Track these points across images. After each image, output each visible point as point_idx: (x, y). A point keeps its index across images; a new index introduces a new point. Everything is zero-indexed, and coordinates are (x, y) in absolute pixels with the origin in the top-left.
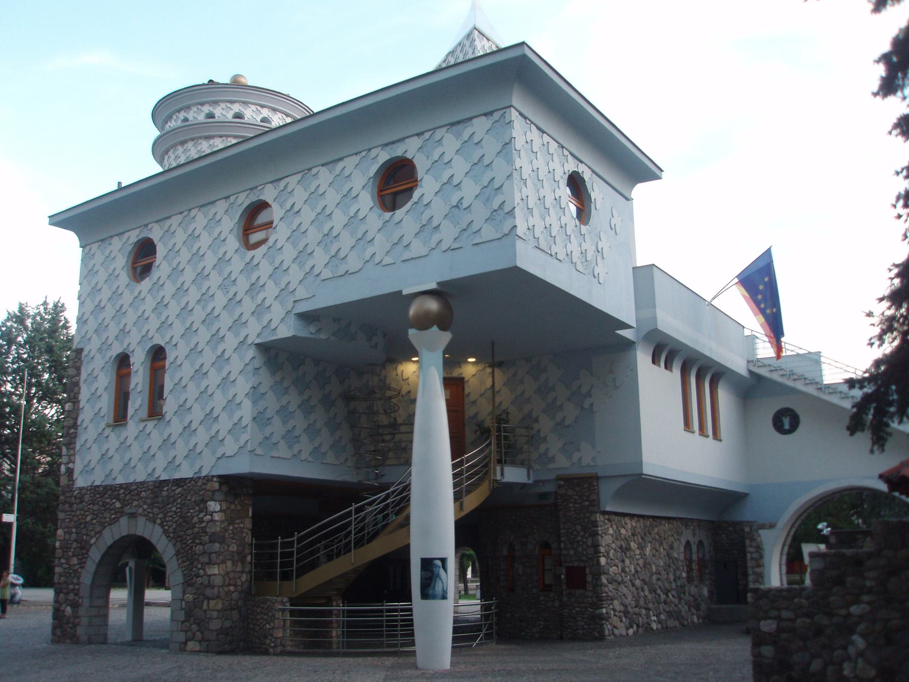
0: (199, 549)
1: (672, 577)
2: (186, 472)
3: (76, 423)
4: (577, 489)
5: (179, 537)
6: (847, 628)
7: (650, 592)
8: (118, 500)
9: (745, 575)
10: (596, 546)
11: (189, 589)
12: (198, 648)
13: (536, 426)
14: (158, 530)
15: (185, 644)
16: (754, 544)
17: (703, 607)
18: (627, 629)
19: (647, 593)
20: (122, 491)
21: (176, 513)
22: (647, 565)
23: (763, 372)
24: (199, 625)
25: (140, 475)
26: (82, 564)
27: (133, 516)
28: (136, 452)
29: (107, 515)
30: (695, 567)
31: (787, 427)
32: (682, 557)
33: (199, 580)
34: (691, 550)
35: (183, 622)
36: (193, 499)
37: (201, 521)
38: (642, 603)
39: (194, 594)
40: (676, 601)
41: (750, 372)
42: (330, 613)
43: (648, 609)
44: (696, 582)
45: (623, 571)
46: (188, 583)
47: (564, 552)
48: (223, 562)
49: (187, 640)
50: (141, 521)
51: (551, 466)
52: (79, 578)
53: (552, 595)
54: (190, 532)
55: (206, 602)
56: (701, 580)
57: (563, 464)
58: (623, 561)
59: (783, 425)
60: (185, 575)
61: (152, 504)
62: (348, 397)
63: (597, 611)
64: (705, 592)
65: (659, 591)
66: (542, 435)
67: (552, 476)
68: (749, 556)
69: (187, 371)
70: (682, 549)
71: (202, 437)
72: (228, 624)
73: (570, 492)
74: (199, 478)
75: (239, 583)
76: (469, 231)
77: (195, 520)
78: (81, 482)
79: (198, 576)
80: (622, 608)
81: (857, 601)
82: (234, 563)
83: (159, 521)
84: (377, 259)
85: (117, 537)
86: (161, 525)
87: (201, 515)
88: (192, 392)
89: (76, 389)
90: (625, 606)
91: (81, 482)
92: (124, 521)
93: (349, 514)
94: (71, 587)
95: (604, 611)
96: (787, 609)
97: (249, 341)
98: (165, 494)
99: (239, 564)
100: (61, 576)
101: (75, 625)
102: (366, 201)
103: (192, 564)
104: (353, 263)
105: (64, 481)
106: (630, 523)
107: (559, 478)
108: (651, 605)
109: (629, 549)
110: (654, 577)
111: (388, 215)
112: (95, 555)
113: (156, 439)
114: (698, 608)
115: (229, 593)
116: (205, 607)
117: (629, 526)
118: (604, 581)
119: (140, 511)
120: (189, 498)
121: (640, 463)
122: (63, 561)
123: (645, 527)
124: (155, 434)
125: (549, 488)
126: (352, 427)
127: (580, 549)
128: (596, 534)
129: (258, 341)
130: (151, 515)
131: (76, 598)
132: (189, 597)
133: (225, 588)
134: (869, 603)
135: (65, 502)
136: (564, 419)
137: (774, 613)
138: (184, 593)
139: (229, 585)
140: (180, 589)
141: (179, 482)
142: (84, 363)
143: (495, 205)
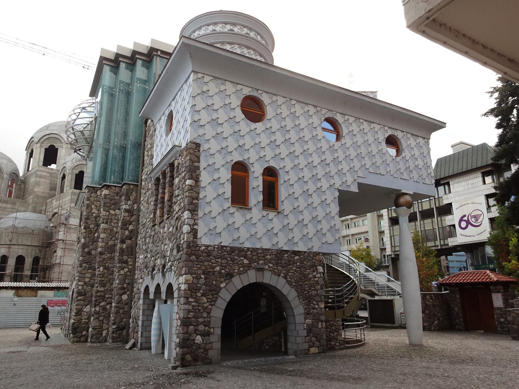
0: (314, 293)
2: (301, 247)
5: (300, 285)
12: (317, 352)
15: (308, 350)
20: (249, 253)
24: (316, 337)
25: (266, 244)
26: (213, 302)
27: (260, 270)
35: (305, 337)
36: (308, 264)
37: (315, 277)
39: (312, 319)
46: (307, 314)
49: (310, 347)
52: (209, 313)
55: (320, 323)
60: (305, 309)
61: (277, 264)
74: (311, 252)
77: (311, 276)
79: (314, 308)
83: (282, 275)
86: (285, 277)
87: (315, 274)
94: (201, 320)
101: (206, 350)
103: (309, 301)
119: (267, 267)
120: (305, 263)
124: (275, 220)
129: (340, 188)
130: (276, 271)
131: (207, 328)
138: (305, 319)
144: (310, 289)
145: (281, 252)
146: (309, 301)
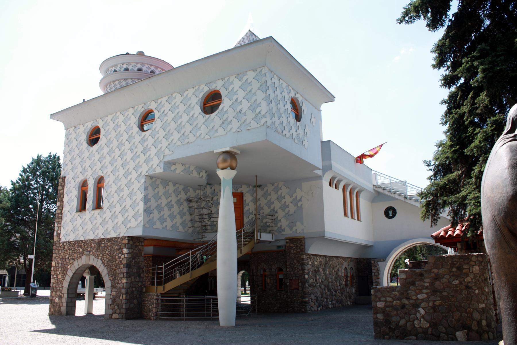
1: (338, 284)
2: (113, 235)
3: (62, 212)
4: (295, 244)
6: (416, 306)
7: (328, 291)
8: (81, 247)
9: (372, 283)
10: (303, 270)
11: (114, 290)
12: (118, 317)
13: (276, 215)
14: (100, 262)
15: (112, 315)
16: (375, 269)
17: (353, 297)
18: (318, 308)
19: (327, 291)
21: (108, 254)
22: (327, 278)
23: (380, 190)
26: (64, 278)
28: (90, 226)
29: (76, 255)
30: (349, 279)
31: (391, 215)
32: (343, 275)
33: (119, 286)
34: (347, 272)
37: (120, 258)
38: (324, 295)
40: (340, 295)
41: (374, 190)
42: (180, 301)
43: (327, 299)
44: (349, 286)
45: (316, 281)
46: (113, 287)
47: (289, 273)
48: (130, 277)
50: (92, 257)
51: (283, 233)
53: (283, 292)
54: (114, 263)
56: (352, 286)
57: (288, 233)
58: (316, 277)
59: (389, 215)
60: (112, 283)
62: (189, 201)
63: (304, 300)
64: (354, 291)
65: (332, 290)
66: (279, 219)
67: (284, 238)
68: (373, 274)
69: (114, 188)
70: (343, 271)
71: (120, 219)
72: (132, 306)
73: (292, 245)
74: (119, 238)
75: (137, 286)
76: (245, 124)
77: (117, 257)
78: (63, 240)
79: (118, 283)
80: (315, 298)
81: (421, 293)
82: (135, 278)
83: (100, 258)
84: (202, 137)
85: (80, 265)
86: (102, 260)
87: (120, 255)
88: (116, 198)
89: (62, 196)
90: (317, 297)
91: (63, 240)
92: (84, 257)
93: (189, 255)
95: (307, 299)
96: (389, 296)
97: (143, 174)
98: (103, 245)
99: (138, 278)
100: (53, 283)
102: (198, 110)
103: (115, 278)
104: (192, 138)
105: (56, 239)
106: (319, 259)
107: (286, 239)
108: (329, 297)
109: (319, 271)
110: (330, 284)
111: (208, 116)
112: (70, 273)
113: (99, 220)
114: (350, 298)
115: (132, 292)
116: (121, 298)
117: (319, 261)
118: (307, 285)
121: (324, 232)
122: (55, 276)
123: (326, 261)
125: (283, 243)
126: (191, 214)
127: (296, 271)
128: (303, 264)
129: (147, 174)
132: (114, 293)
133: (131, 289)
134: (426, 293)
135: (55, 250)
136: (267, 191)
137: (383, 299)
139: (133, 288)
140: (109, 289)
141: (110, 240)
142: (66, 184)
143: (257, 112)
144: (116, 267)
145: (101, 241)
146: (115, 278)
